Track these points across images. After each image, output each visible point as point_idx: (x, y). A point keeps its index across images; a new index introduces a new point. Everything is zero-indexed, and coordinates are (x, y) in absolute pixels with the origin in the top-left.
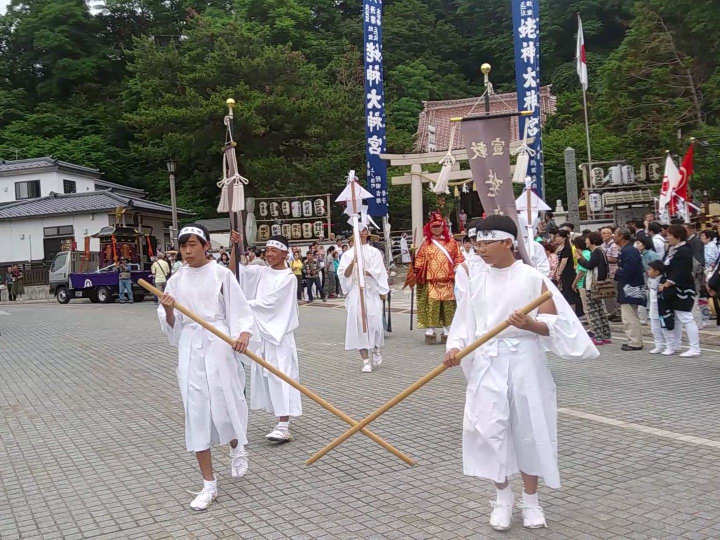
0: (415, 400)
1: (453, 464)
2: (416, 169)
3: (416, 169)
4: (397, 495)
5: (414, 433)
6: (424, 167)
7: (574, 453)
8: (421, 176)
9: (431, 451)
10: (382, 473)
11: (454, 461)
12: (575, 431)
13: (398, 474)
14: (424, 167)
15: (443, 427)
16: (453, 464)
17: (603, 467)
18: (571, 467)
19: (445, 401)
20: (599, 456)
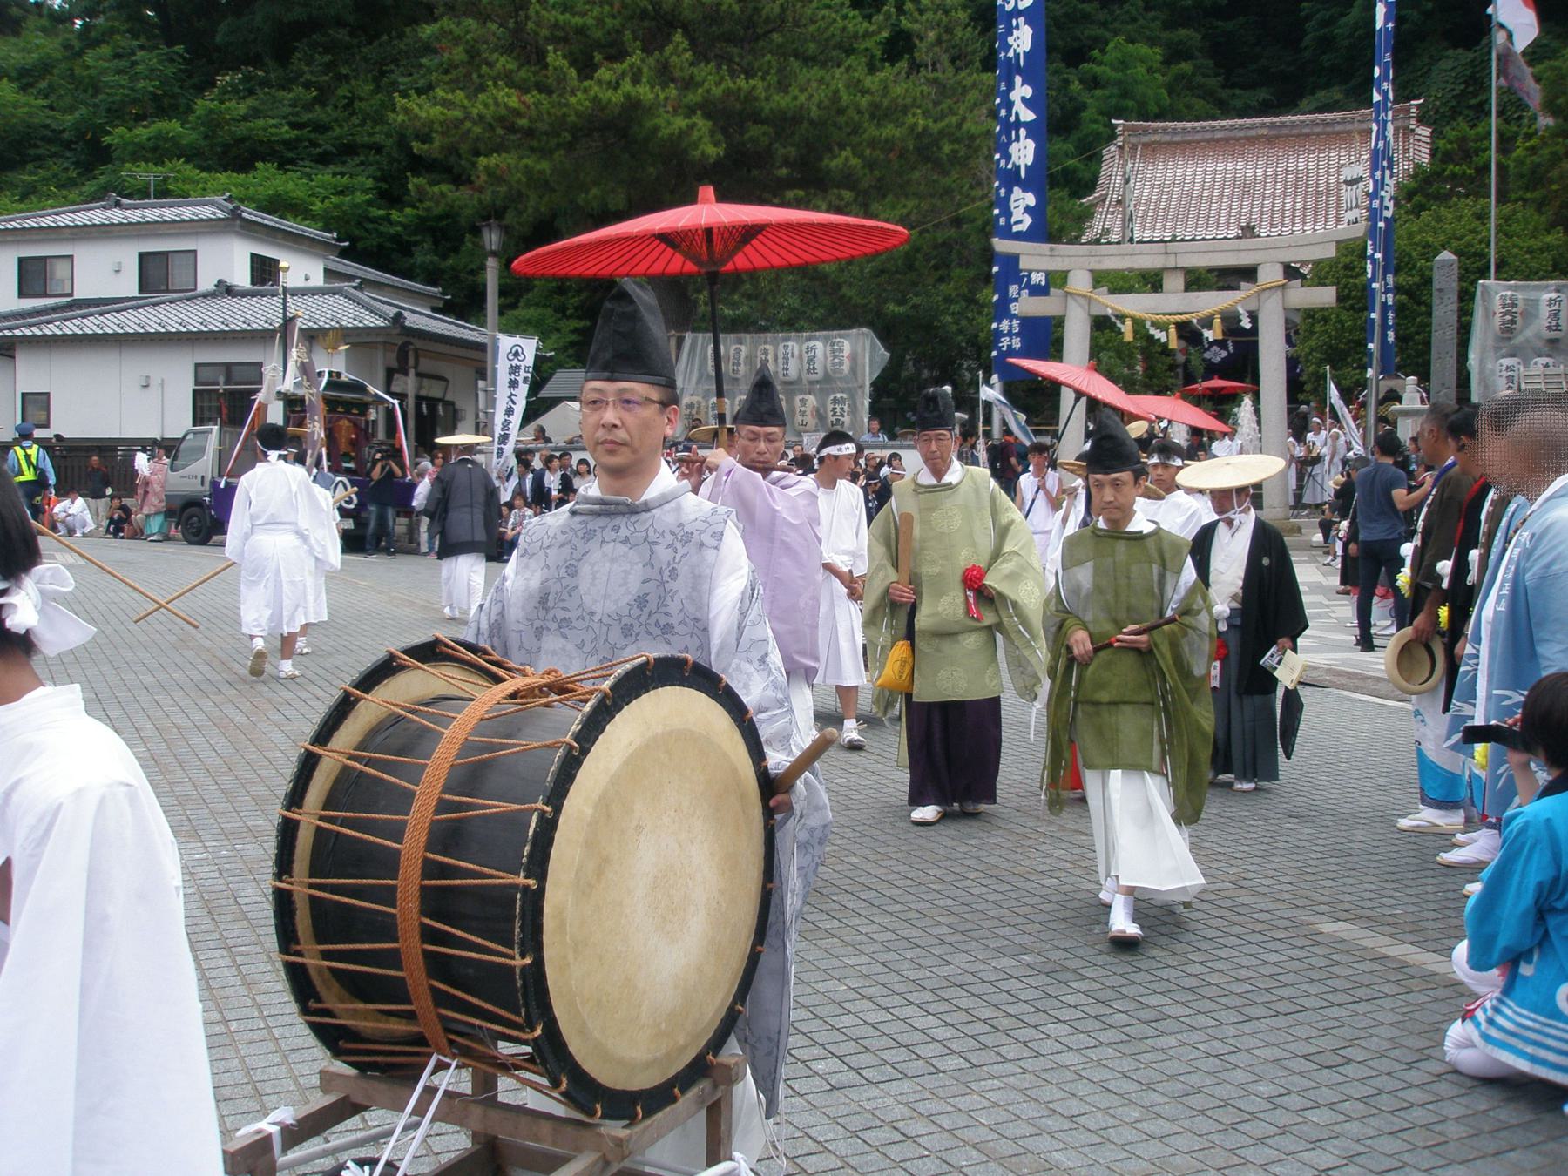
0: (973, 875)
1: (1025, 1071)
2: (1080, 282)
3: (1080, 282)
4: (853, 1161)
5: (946, 971)
6: (1099, 278)
7: (1348, 1061)
8: (1089, 299)
9: (980, 1027)
10: (833, 1088)
11: (1028, 1064)
12: (1360, 993)
13: (873, 1092)
14: (1099, 278)
15: (1027, 958)
16: (1025, 1071)
17: (1417, 1115)
18: (1330, 1106)
19: (1047, 882)
20: (1413, 1076)
